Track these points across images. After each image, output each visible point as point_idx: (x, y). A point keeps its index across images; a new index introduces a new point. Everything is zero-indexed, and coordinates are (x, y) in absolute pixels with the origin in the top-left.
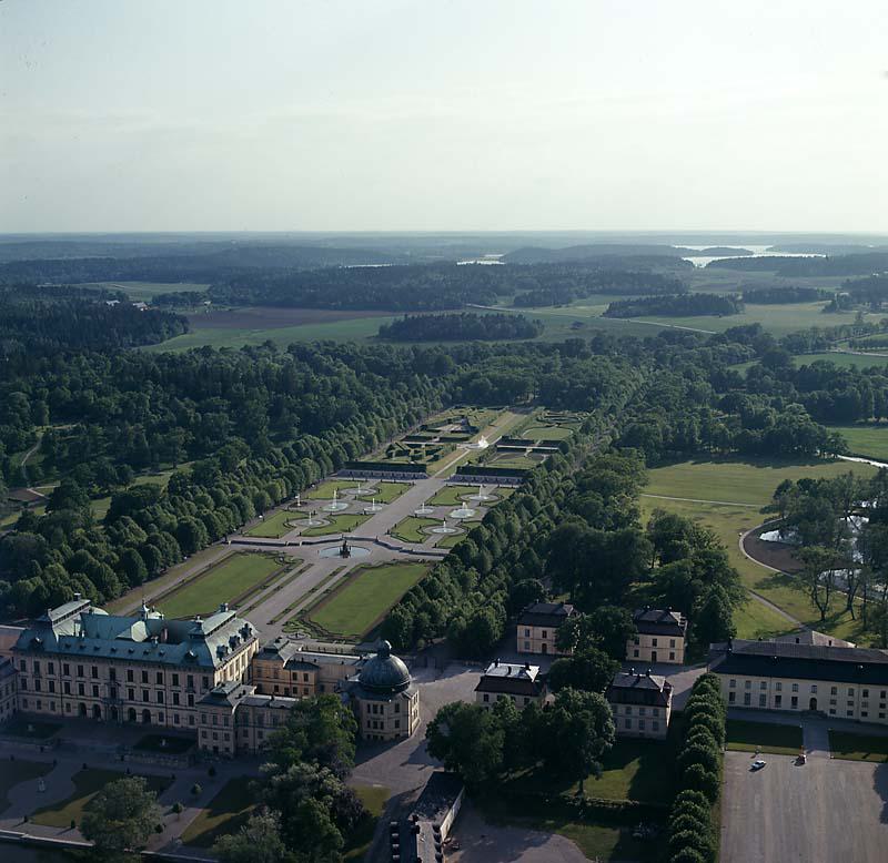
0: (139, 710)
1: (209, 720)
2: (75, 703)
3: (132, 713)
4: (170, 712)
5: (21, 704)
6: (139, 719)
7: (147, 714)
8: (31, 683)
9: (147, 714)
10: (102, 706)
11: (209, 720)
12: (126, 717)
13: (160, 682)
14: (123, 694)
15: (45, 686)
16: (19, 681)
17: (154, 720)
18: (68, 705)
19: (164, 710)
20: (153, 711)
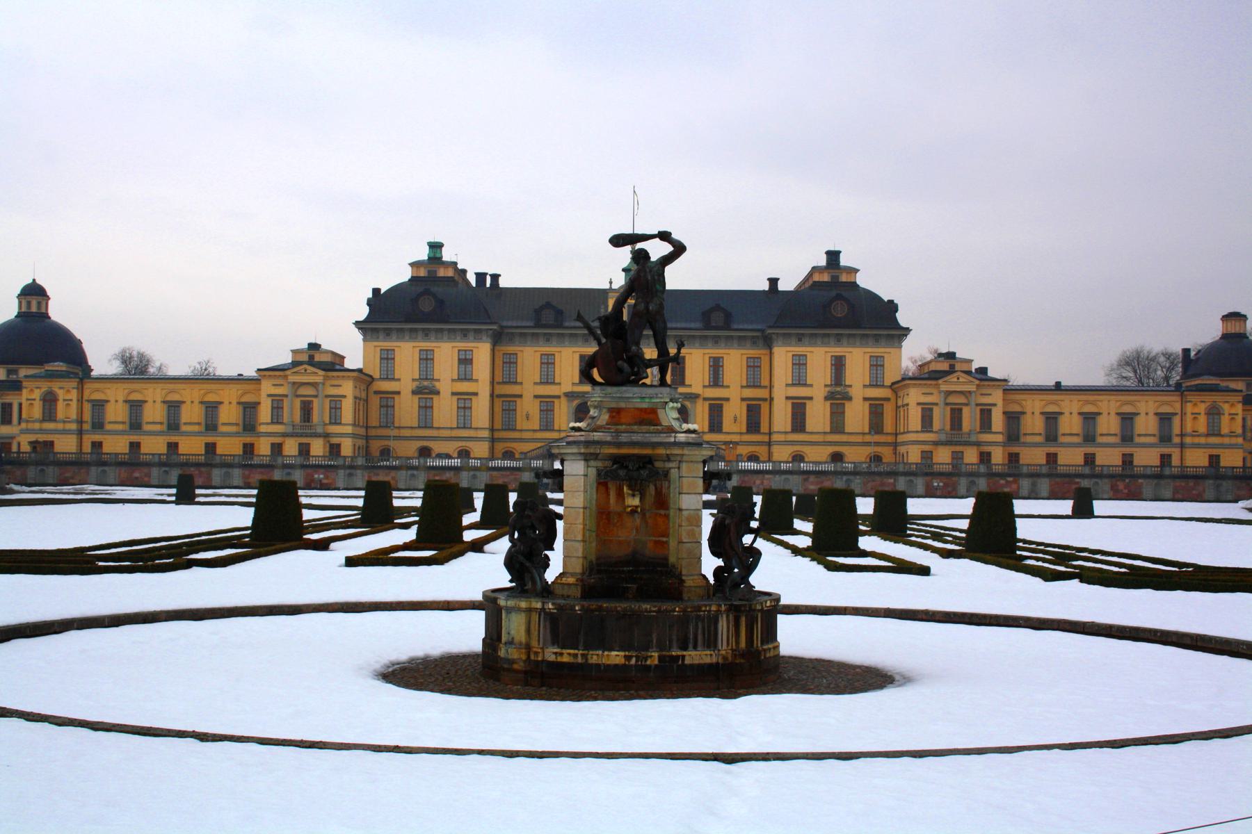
16: (375, 401)
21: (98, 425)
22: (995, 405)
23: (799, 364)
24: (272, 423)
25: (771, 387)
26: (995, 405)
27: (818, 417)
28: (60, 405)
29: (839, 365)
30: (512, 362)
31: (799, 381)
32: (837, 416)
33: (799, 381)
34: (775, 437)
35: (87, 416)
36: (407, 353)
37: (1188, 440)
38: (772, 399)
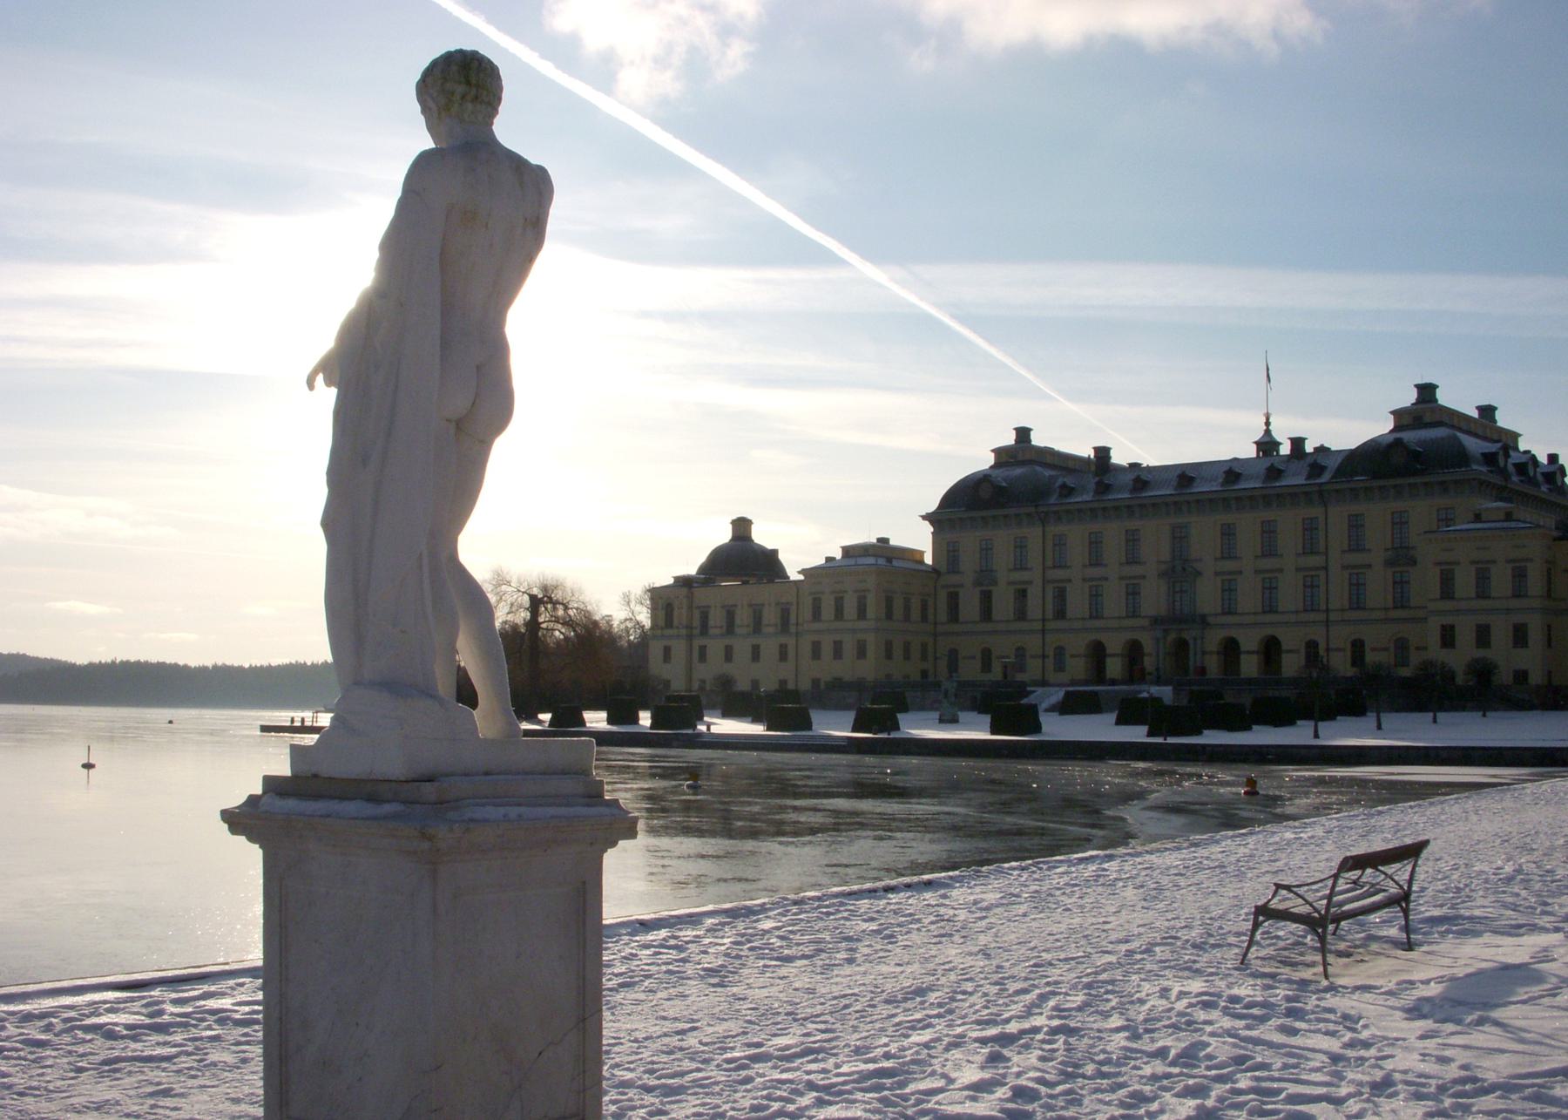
0: (1249, 641)
1: (1465, 582)
2: (1077, 644)
3: (1231, 649)
4: (1341, 637)
5: (943, 664)
6: (1250, 666)
7: (1271, 649)
8: (970, 606)
9: (1271, 649)
10: (1148, 644)
11: (1465, 582)
12: (1213, 665)
13: (1310, 549)
14: (1207, 597)
15: (1003, 604)
16: (943, 595)
17: (1291, 665)
18: (1060, 651)
19: (1318, 634)
20: (1292, 640)
21: (704, 630)
22: (1531, 560)
23: (1355, 524)
24: (1091, 617)
25: (1326, 554)
26: (1531, 560)
27: (1378, 588)
28: (676, 613)
29: (1400, 522)
30: (1060, 542)
31: (1356, 545)
32: (1400, 584)
33: (1356, 545)
34: (1333, 617)
35: (696, 623)
36: (970, 541)
37: (684, 632)
38: (1326, 568)
